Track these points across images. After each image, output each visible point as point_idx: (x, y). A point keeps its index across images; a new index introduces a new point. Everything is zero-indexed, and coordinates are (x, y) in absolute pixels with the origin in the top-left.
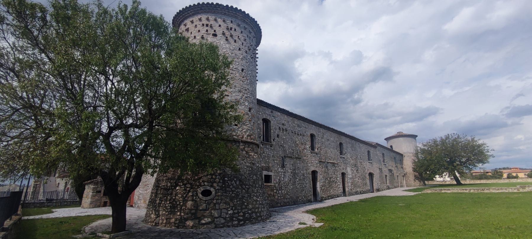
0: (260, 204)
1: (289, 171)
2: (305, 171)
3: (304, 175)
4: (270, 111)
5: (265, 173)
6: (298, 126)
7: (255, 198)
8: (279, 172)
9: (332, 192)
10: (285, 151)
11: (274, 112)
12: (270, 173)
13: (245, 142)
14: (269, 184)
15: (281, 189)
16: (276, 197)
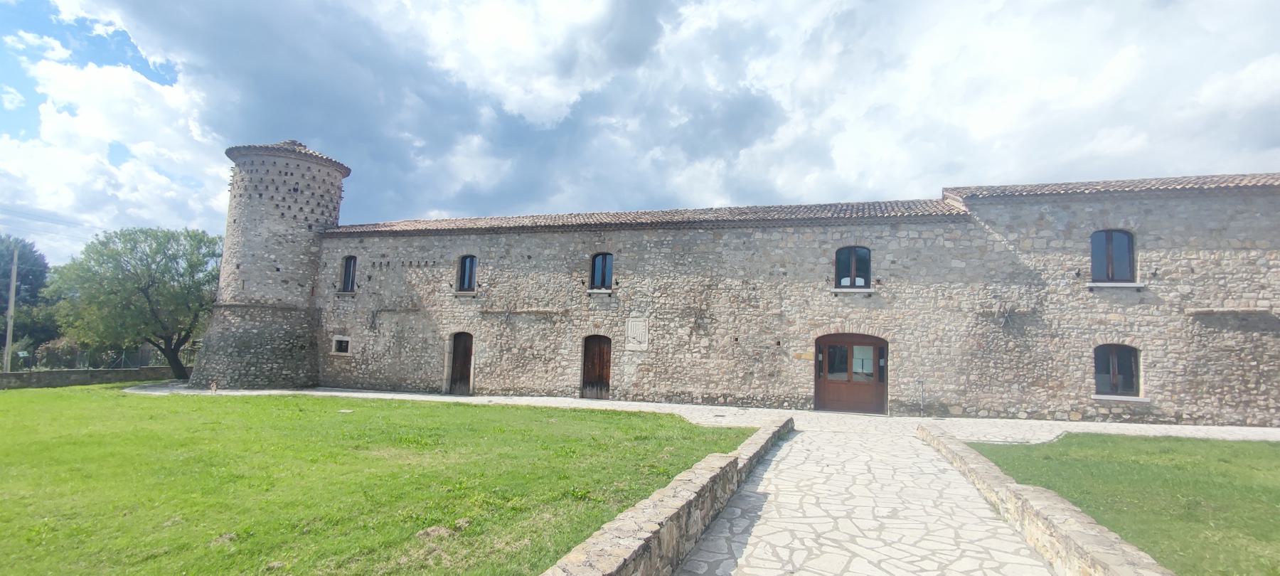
2: (430, 334)
3: (425, 341)
4: (357, 240)
6: (422, 249)
9: (524, 381)
11: (366, 240)
12: (346, 338)
15: (366, 362)
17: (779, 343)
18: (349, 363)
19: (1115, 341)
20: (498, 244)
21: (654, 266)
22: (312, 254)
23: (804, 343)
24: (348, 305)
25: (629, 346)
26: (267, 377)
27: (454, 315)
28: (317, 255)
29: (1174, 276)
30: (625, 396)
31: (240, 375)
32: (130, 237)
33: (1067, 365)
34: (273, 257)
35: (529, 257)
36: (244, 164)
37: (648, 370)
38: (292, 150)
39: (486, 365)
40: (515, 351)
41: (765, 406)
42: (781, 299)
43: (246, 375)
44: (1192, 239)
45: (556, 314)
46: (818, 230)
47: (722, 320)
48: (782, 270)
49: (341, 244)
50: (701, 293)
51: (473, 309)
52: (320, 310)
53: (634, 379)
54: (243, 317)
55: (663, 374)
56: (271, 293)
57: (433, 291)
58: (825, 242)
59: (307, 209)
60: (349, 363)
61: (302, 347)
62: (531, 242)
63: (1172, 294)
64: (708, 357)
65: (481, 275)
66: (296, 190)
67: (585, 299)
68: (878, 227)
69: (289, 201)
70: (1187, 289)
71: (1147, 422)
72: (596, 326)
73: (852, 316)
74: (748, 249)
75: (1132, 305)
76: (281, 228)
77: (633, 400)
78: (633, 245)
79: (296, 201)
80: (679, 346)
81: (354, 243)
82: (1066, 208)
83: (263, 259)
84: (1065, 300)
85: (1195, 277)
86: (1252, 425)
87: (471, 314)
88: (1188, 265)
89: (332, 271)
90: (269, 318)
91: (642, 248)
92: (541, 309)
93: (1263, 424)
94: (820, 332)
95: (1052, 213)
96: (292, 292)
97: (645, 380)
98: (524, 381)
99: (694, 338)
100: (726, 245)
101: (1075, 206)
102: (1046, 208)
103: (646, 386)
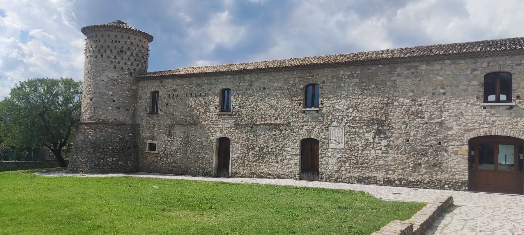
0: (84, 163)
1: (178, 139)
3: (201, 143)
4: (159, 81)
5: (149, 142)
6: (198, 85)
7: (80, 159)
8: (165, 140)
9: (263, 168)
10: (174, 119)
13: (85, 123)
14: (153, 152)
15: (166, 156)
16: (160, 164)
17: (440, 143)
18: (157, 157)
20: (244, 81)
21: (347, 91)
22: (133, 90)
23: (460, 143)
24: (155, 122)
25: (332, 146)
26: (110, 166)
27: (218, 127)
28: (136, 91)
30: (329, 179)
31: (95, 165)
32: (34, 84)
34: (111, 93)
35: (264, 89)
36: (92, 37)
37: (345, 162)
38: (118, 27)
39: (239, 158)
40: (257, 149)
41: (430, 187)
42: (442, 112)
43: (98, 165)
45: (283, 124)
46: (470, 61)
47: (397, 127)
48: (442, 91)
49: (149, 84)
50: (381, 109)
51: (230, 123)
52: (139, 125)
53: (335, 167)
54: (95, 130)
55: (356, 165)
56: (110, 115)
57: (205, 112)
58: (476, 70)
59: (129, 63)
60: (157, 157)
61: (129, 148)
62: (265, 79)
64: (387, 153)
65: (235, 101)
66: (122, 52)
67: (301, 115)
68: (517, 57)
69: (119, 59)
72: (309, 132)
73: (497, 123)
74: (416, 77)
76: (114, 75)
77: (335, 182)
78: (333, 78)
79: (122, 59)
80: (366, 146)
81: (157, 83)
83: (105, 95)
87: (229, 126)
89: (145, 100)
90: (110, 131)
91: (339, 79)
92: (273, 122)
94: (472, 135)
96: (122, 115)
97: (343, 168)
98: (263, 168)
99: (376, 140)
100: (399, 75)
103: (344, 172)
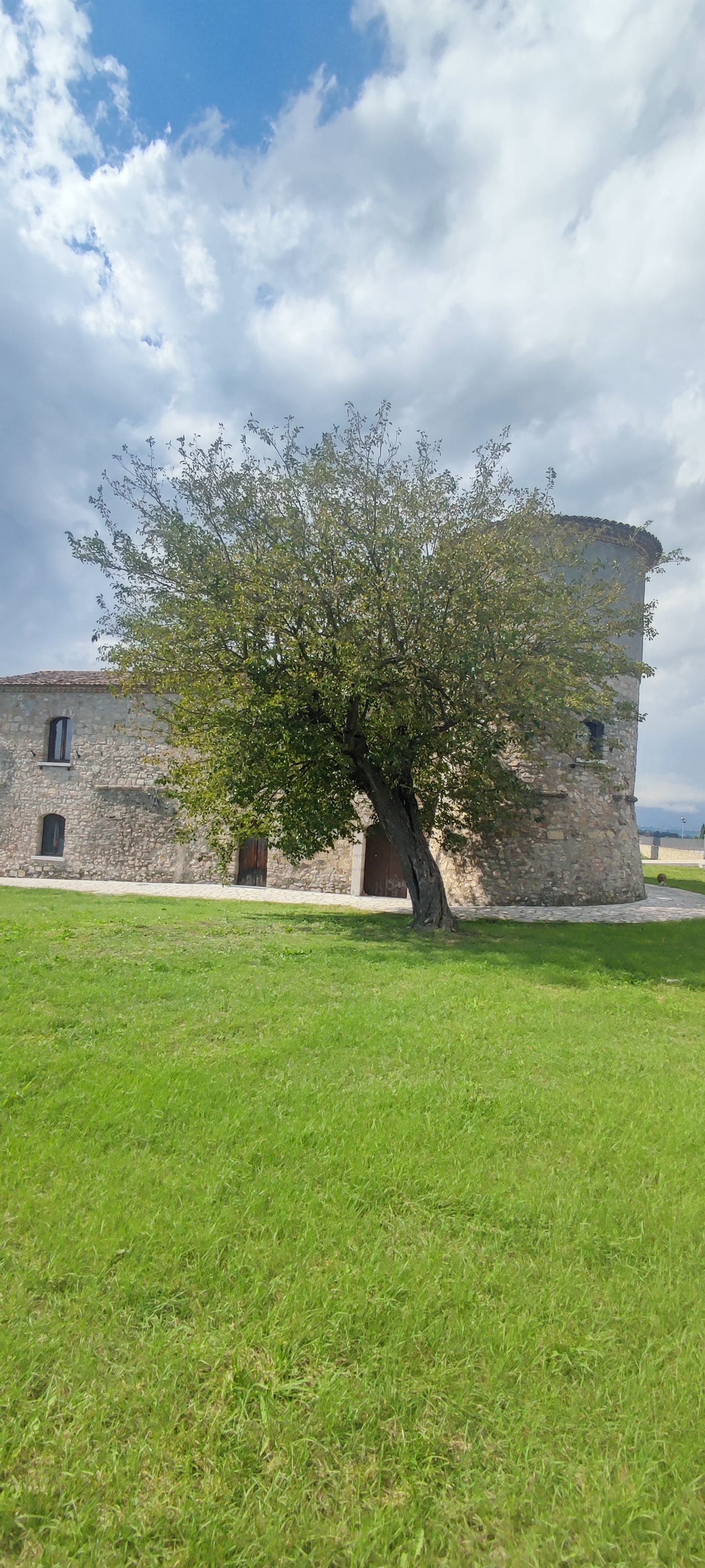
19: (51, 812)
29: (90, 758)
33: (20, 832)
44: (104, 727)
63: (88, 773)
70: (96, 768)
71: (63, 878)
75: (65, 781)
82: (33, 697)
84: (25, 777)
85: (103, 759)
86: (124, 880)
88: (100, 749)
93: (130, 879)
95: (24, 702)
101: (39, 697)
102: (20, 696)
